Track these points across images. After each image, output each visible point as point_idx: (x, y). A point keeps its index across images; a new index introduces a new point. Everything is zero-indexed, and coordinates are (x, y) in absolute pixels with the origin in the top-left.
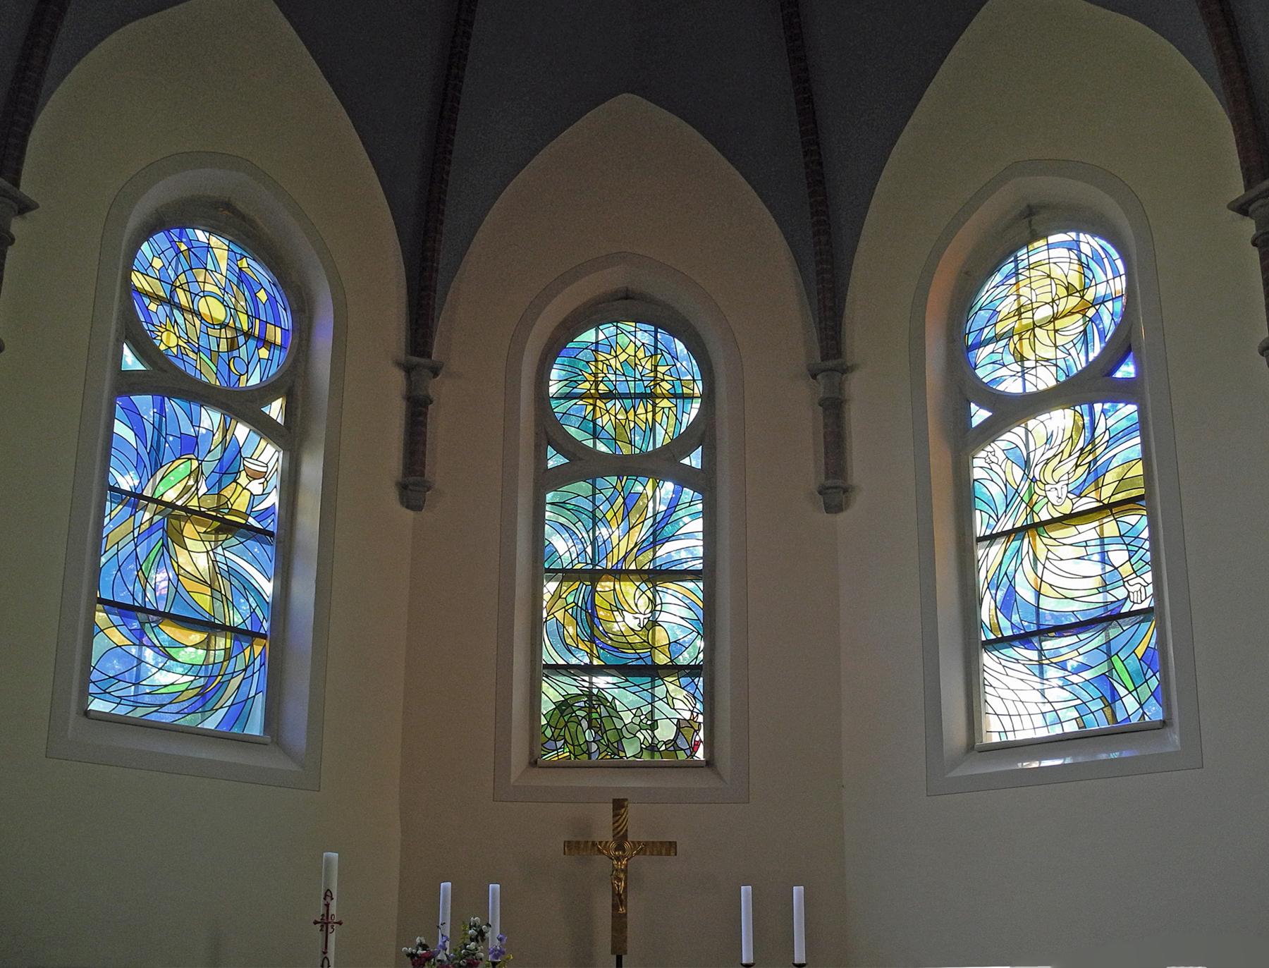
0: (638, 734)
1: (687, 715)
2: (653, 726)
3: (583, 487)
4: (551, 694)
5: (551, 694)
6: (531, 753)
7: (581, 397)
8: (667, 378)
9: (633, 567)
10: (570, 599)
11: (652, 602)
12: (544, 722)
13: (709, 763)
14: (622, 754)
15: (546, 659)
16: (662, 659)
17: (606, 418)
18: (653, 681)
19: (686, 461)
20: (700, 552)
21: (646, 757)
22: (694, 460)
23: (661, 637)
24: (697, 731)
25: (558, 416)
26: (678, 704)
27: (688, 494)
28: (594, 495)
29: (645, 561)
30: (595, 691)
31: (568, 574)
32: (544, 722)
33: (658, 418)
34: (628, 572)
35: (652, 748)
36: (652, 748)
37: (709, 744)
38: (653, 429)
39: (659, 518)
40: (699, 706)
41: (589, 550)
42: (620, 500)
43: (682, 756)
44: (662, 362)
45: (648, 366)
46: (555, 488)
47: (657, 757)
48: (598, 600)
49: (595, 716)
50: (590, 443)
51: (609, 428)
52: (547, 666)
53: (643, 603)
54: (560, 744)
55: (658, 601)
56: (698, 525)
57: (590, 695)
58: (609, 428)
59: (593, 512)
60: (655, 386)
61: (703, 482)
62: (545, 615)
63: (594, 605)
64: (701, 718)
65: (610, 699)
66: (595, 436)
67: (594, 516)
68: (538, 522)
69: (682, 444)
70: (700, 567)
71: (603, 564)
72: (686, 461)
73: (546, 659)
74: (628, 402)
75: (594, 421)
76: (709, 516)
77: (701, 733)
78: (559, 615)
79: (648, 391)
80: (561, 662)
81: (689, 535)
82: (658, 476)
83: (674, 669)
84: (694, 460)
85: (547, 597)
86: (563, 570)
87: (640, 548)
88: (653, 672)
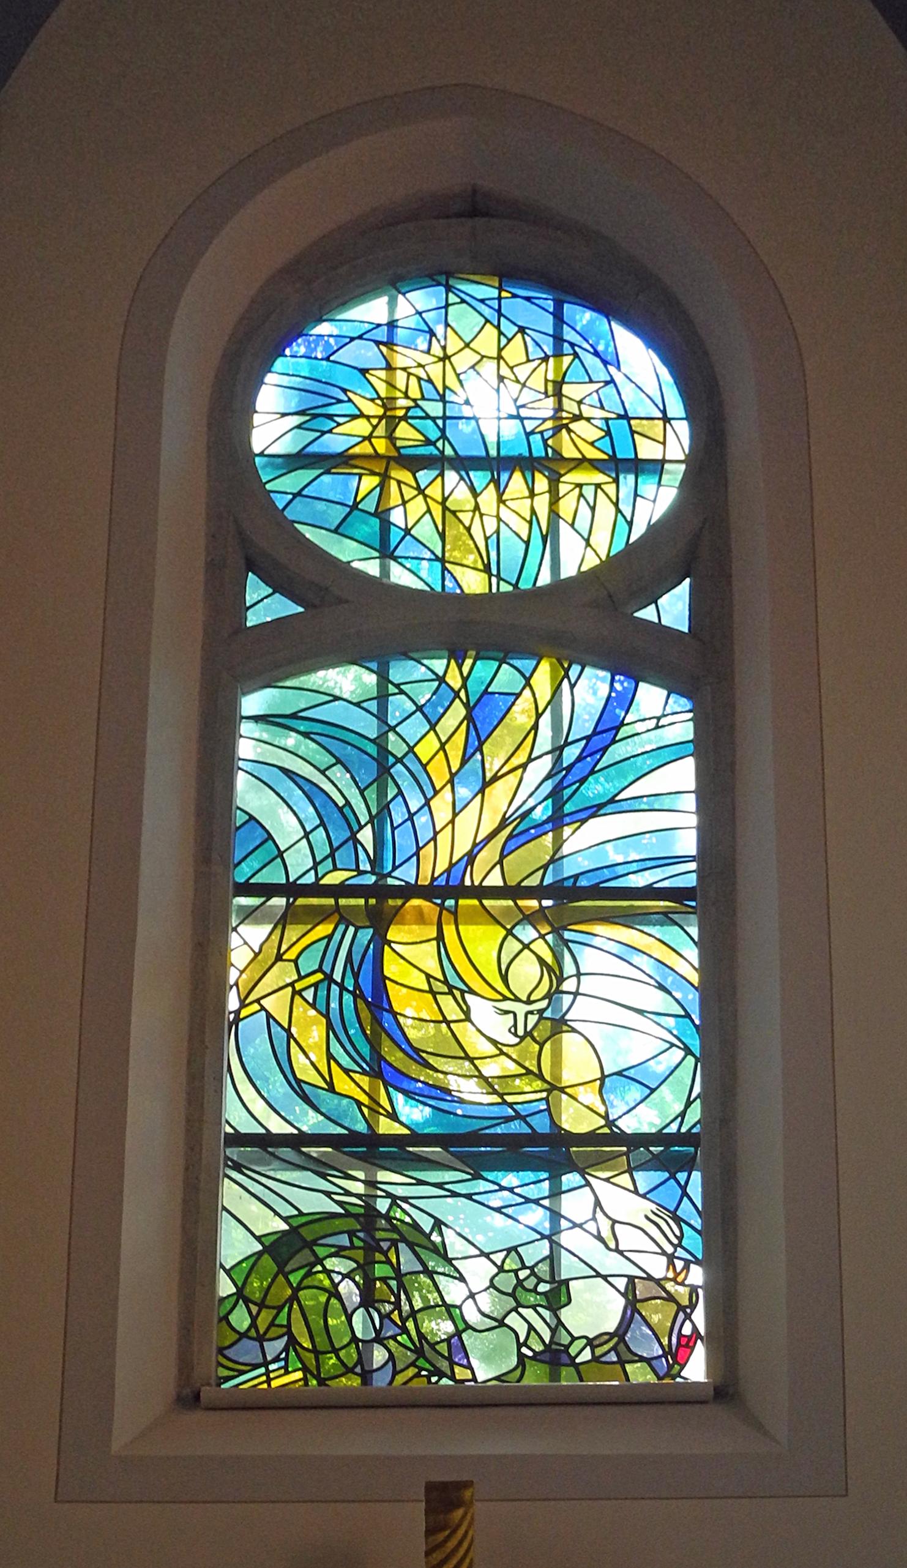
0: (513, 1320)
1: (657, 1267)
2: (557, 1296)
3: (350, 680)
4: (248, 1218)
5: (248, 1218)
6: (185, 1364)
7: (342, 461)
8: (587, 411)
9: (495, 880)
10: (309, 964)
11: (554, 972)
12: (226, 1287)
13: (723, 1390)
14: (461, 1373)
15: (236, 1117)
16: (576, 1119)
17: (417, 506)
18: (555, 1179)
19: (648, 614)
20: (687, 843)
21: (535, 1377)
22: (674, 608)
23: (576, 1062)
24: (686, 1310)
25: (280, 501)
26: (629, 1238)
27: (650, 698)
28: (382, 698)
29: (526, 864)
30: (383, 1205)
31: (298, 901)
32: (226, 1287)
33: (566, 507)
34: (481, 892)
35: (555, 1355)
36: (555, 1355)
37: (724, 1339)
38: (551, 537)
39: (571, 754)
40: (694, 1242)
41: (366, 836)
42: (458, 711)
43: (638, 1374)
44: (577, 370)
45: (537, 381)
46: (269, 676)
47: (567, 1379)
48: (392, 967)
49: (381, 1270)
50: (372, 568)
51: (426, 531)
52: (238, 1139)
53: (526, 974)
54: (274, 1348)
55: (569, 968)
56: (684, 774)
57: (370, 1215)
58: (426, 531)
59: (380, 742)
60: (557, 430)
61: (698, 667)
62: (233, 1003)
63: (380, 980)
64: (697, 1276)
65: (426, 1224)
66: (386, 553)
67: (384, 751)
68: (215, 763)
69: (637, 570)
70: (691, 881)
71: (406, 874)
72: (648, 614)
73: (236, 1117)
74: (479, 478)
75: (382, 515)
76: (717, 754)
77: (699, 1316)
78: (276, 1005)
79: (538, 451)
80: (277, 1126)
81: (652, 803)
82: (571, 651)
83: (611, 1147)
84: (674, 608)
85: (239, 957)
86: (291, 889)
87: (517, 830)
88: (556, 1153)
